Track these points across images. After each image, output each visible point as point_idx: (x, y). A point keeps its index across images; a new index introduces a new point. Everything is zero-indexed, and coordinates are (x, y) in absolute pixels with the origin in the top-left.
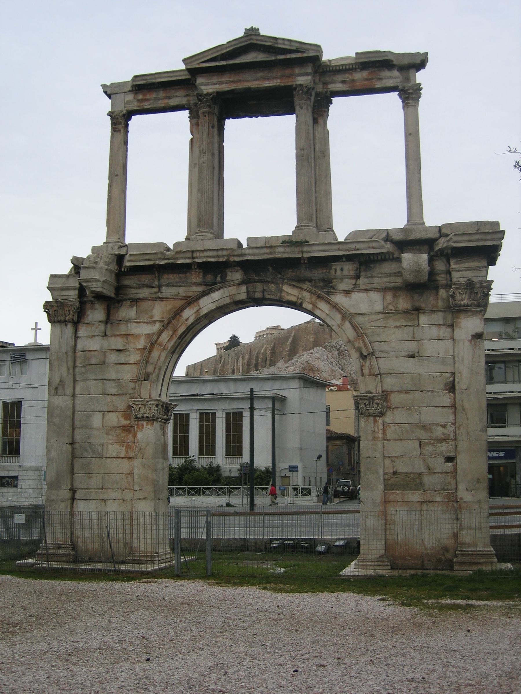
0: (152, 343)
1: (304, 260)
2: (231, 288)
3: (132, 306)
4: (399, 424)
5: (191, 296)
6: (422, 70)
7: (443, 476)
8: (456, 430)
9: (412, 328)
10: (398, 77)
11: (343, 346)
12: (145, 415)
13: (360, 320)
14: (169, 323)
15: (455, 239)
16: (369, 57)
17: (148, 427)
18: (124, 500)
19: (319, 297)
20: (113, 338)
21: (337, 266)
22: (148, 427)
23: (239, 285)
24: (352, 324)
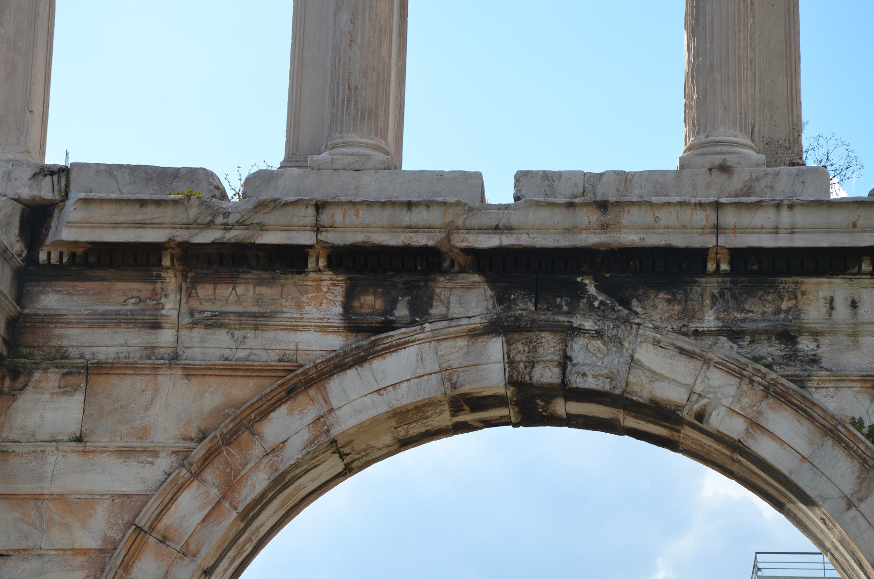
2: (445, 344)
3: (66, 390)
5: (301, 366)
23: (474, 334)
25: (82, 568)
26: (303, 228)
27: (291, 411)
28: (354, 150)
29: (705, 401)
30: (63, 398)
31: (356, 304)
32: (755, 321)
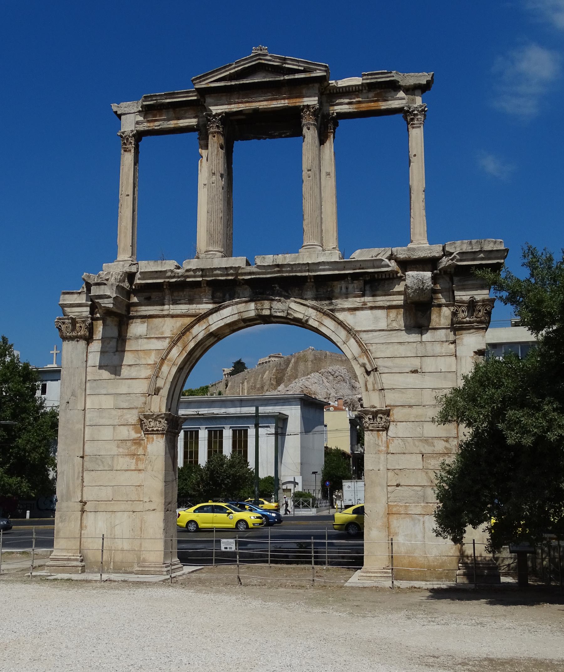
0: (162, 358)
1: (311, 279)
4: (402, 438)
6: (427, 92)
9: (415, 344)
10: (403, 99)
11: (337, 372)
12: (155, 429)
13: (364, 336)
17: (158, 440)
18: (134, 512)
19: (325, 314)
21: (343, 284)
22: (158, 440)
24: (356, 341)
25: (150, 369)
27: (199, 326)
28: (212, 252)
31: (215, 295)
32: (321, 294)
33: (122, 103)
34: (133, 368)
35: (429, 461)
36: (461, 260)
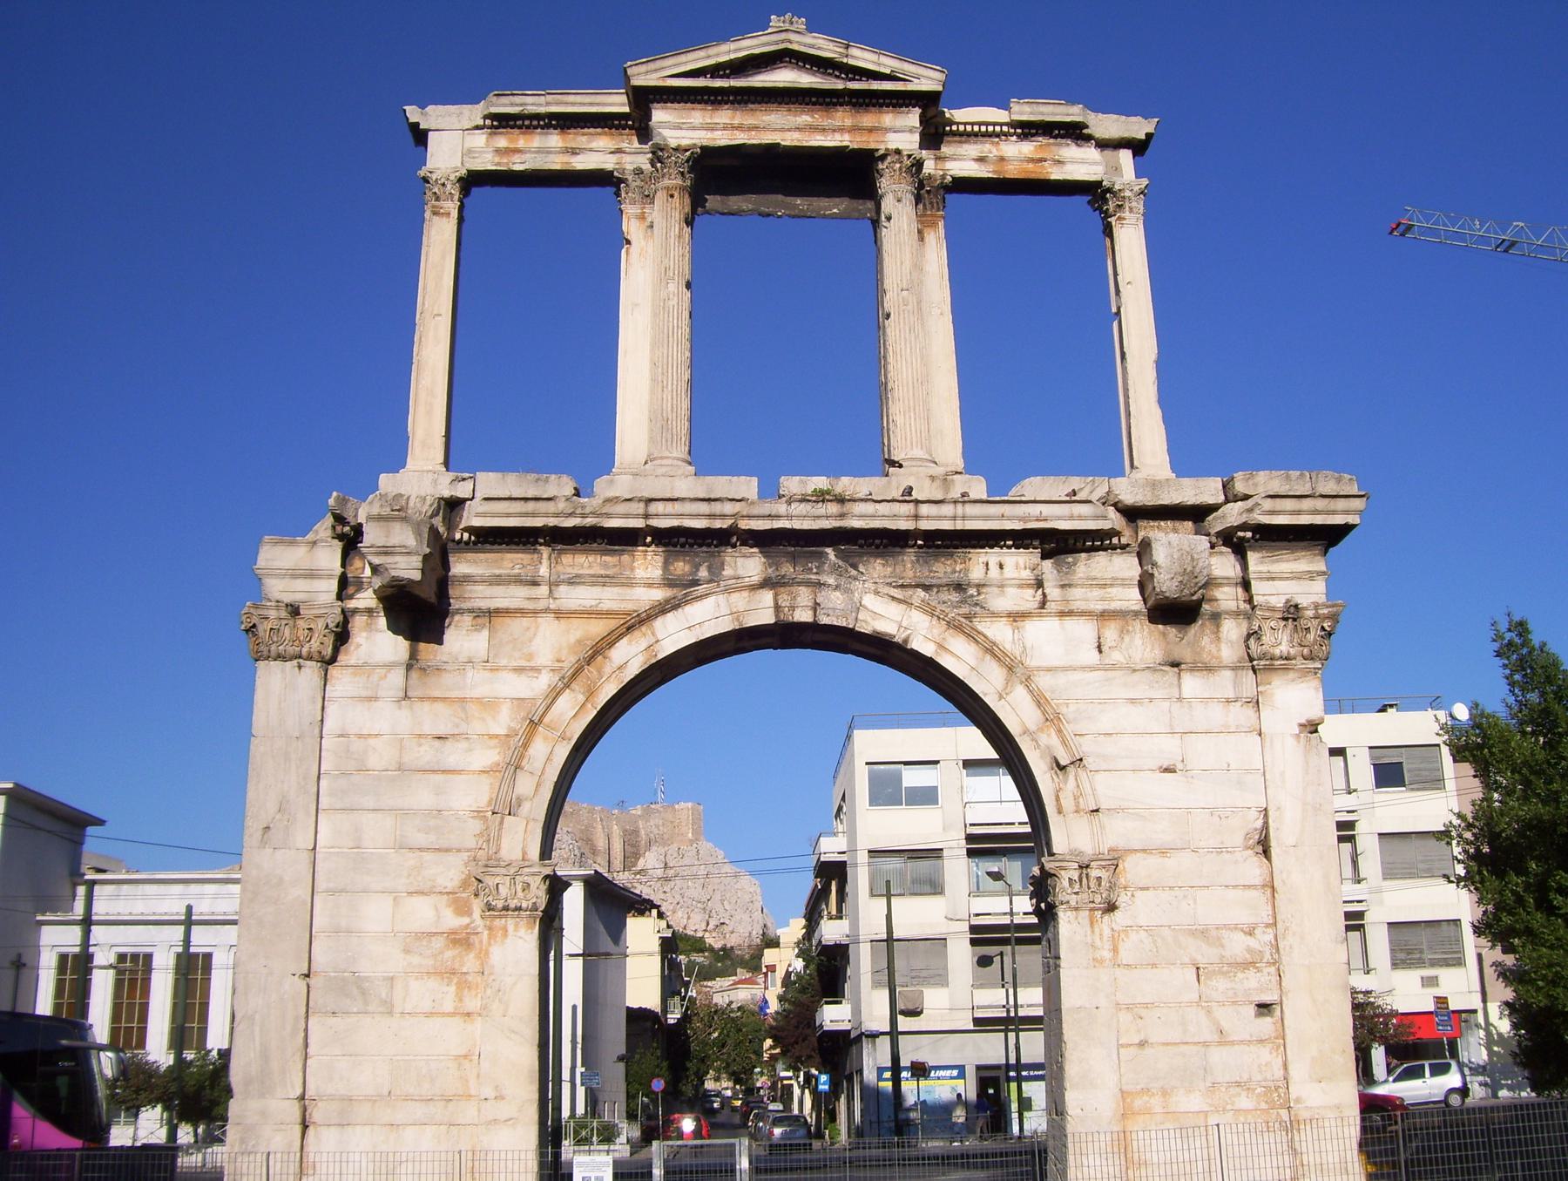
3: (477, 628)
4: (1148, 930)
7: (1253, 1048)
8: (1276, 940)
9: (1166, 704)
14: (577, 672)
15: (1268, 504)
16: (1042, 114)
17: (519, 934)
20: (427, 706)
21: (992, 556)
23: (754, 588)
25: (495, 747)
26: (636, 516)
27: (630, 641)
29: (909, 632)
30: (476, 633)
31: (672, 568)
33: (430, 108)
34: (448, 743)
35: (1214, 983)
36: (1272, 513)
